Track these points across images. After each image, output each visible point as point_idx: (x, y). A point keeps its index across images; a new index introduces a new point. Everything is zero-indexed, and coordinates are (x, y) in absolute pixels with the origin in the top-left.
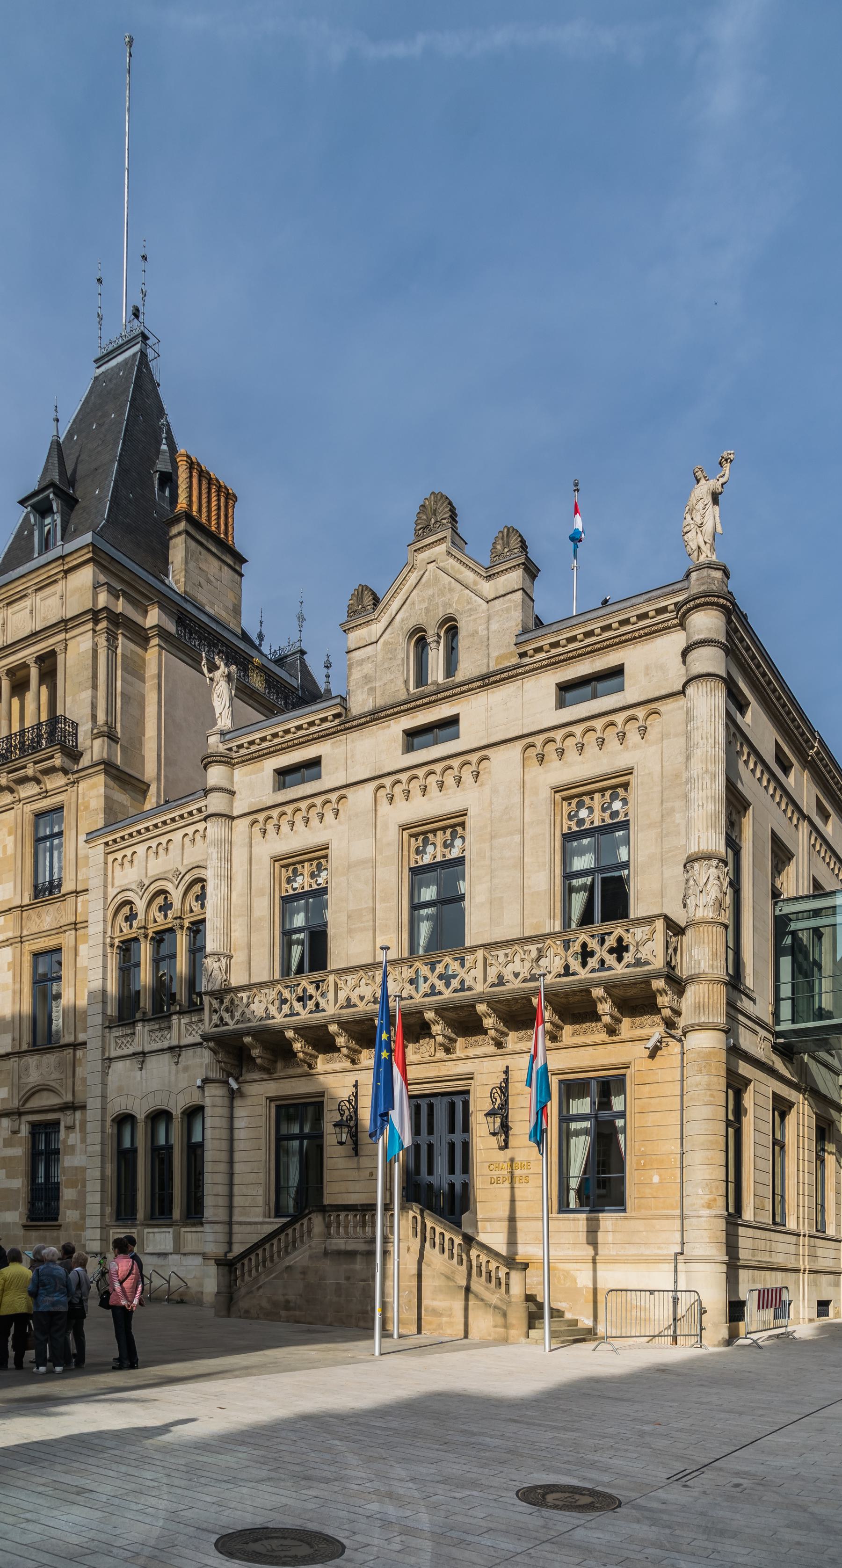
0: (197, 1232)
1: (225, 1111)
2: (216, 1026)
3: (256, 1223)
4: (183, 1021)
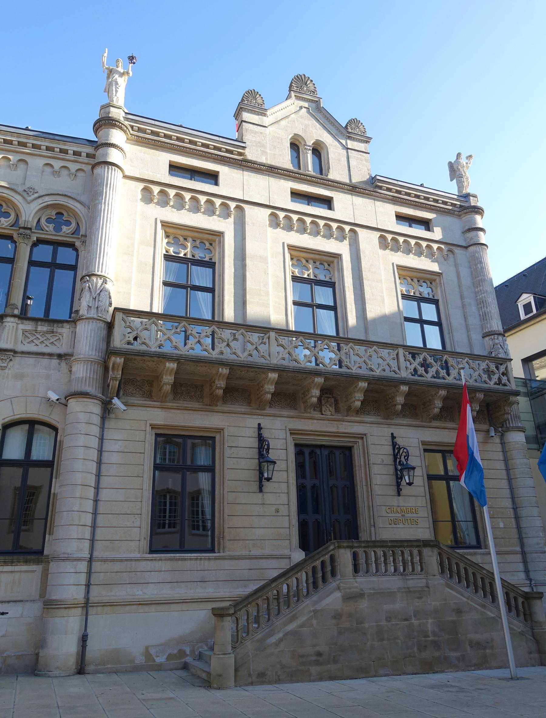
0: (12, 572)
1: (96, 430)
2: (129, 343)
3: (131, 560)
4: (21, 327)
